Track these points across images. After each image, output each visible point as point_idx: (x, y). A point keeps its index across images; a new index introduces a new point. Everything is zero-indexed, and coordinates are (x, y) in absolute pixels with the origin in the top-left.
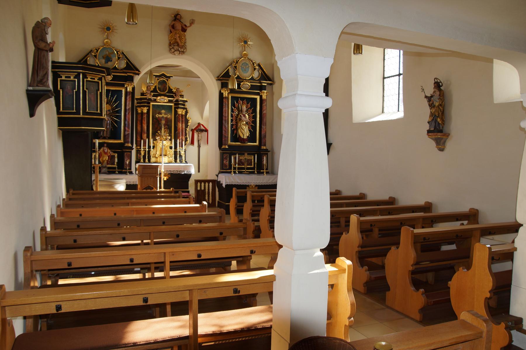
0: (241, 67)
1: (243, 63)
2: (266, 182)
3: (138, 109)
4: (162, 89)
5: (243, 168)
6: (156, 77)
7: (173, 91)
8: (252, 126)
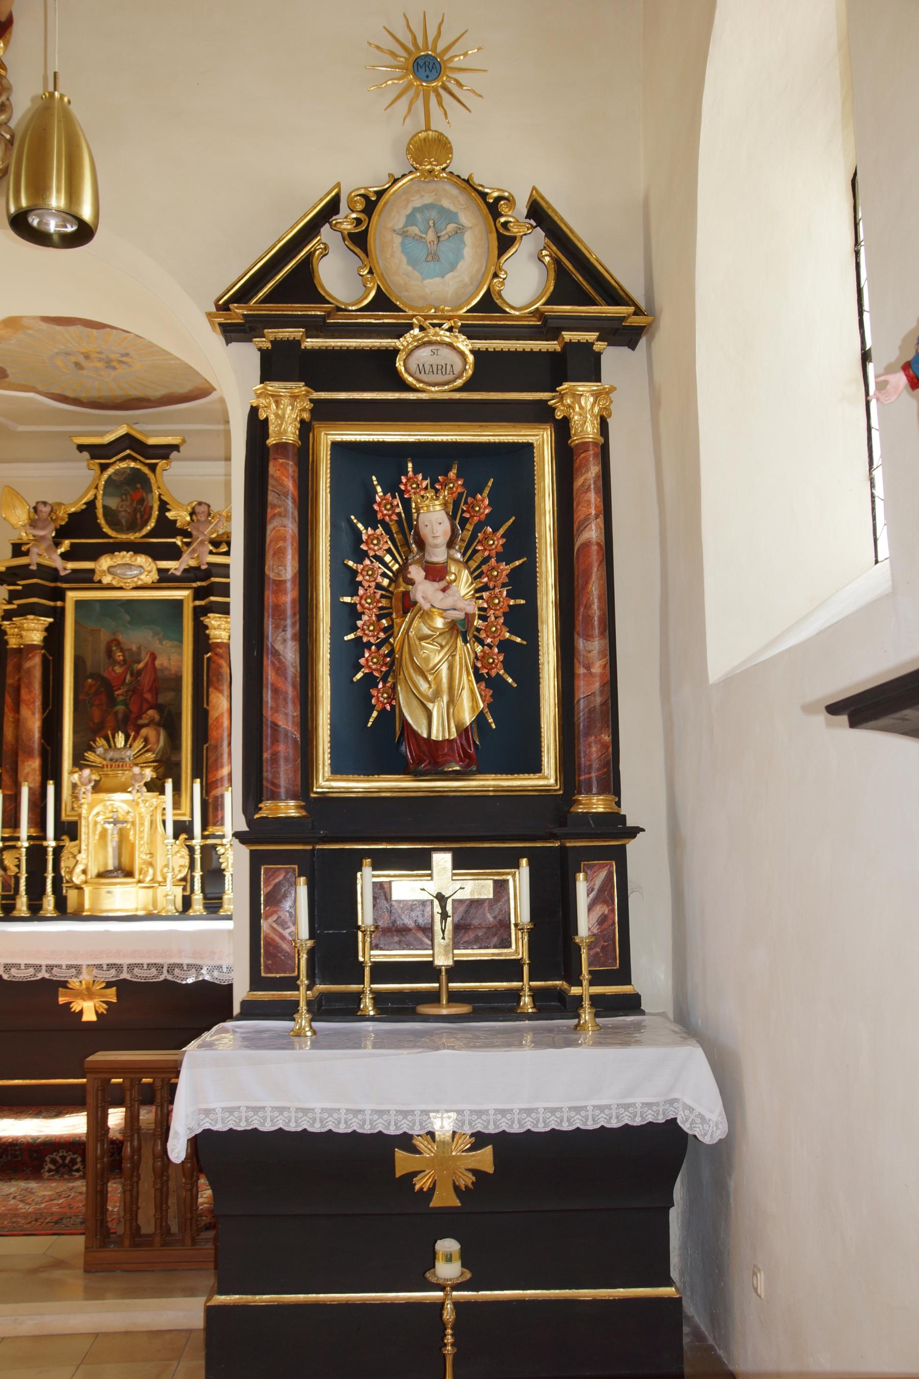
0: (404, 234)
1: (415, 210)
2: (565, 1105)
3: (9, 631)
4: (124, 517)
5: (426, 970)
6: (93, 457)
7: (175, 521)
8: (504, 646)
